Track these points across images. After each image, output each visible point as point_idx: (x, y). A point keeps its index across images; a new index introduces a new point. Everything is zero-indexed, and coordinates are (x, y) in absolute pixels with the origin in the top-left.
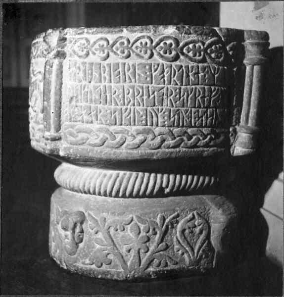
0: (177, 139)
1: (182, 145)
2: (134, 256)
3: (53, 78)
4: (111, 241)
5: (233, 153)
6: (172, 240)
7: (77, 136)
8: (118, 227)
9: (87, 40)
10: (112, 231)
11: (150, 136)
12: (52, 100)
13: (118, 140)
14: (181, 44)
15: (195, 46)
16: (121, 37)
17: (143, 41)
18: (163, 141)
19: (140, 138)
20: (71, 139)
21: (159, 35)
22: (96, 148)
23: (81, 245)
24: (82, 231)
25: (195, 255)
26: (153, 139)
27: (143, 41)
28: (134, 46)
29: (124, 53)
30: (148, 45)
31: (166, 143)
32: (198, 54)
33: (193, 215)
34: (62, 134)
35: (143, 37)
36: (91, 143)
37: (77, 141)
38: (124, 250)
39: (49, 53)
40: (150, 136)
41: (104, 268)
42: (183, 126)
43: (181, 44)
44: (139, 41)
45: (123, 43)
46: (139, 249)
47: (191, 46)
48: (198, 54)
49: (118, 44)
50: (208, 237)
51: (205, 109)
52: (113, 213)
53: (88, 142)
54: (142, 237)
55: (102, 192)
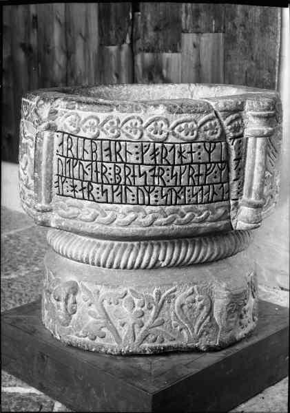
0: (169, 217)
1: (175, 222)
2: (129, 331)
3: (44, 149)
5: (235, 227)
6: (169, 314)
7: (68, 210)
8: (112, 301)
10: (106, 304)
11: (141, 214)
12: (43, 172)
13: (109, 216)
15: (187, 126)
16: (112, 117)
18: (155, 219)
19: (132, 215)
20: (61, 211)
21: (150, 115)
23: (75, 316)
26: (144, 217)
27: (134, 121)
28: (125, 125)
29: (113, 132)
30: (138, 126)
31: (158, 221)
32: (190, 134)
33: (193, 289)
34: (53, 205)
35: (133, 117)
37: (69, 215)
39: (40, 125)
40: (141, 214)
41: (98, 341)
42: (176, 204)
43: (172, 125)
44: (129, 122)
46: (134, 324)
47: (183, 125)
48: (190, 134)
49: (108, 124)
50: (210, 311)
51: (200, 187)
53: (79, 217)
54: (137, 312)
55: (95, 262)
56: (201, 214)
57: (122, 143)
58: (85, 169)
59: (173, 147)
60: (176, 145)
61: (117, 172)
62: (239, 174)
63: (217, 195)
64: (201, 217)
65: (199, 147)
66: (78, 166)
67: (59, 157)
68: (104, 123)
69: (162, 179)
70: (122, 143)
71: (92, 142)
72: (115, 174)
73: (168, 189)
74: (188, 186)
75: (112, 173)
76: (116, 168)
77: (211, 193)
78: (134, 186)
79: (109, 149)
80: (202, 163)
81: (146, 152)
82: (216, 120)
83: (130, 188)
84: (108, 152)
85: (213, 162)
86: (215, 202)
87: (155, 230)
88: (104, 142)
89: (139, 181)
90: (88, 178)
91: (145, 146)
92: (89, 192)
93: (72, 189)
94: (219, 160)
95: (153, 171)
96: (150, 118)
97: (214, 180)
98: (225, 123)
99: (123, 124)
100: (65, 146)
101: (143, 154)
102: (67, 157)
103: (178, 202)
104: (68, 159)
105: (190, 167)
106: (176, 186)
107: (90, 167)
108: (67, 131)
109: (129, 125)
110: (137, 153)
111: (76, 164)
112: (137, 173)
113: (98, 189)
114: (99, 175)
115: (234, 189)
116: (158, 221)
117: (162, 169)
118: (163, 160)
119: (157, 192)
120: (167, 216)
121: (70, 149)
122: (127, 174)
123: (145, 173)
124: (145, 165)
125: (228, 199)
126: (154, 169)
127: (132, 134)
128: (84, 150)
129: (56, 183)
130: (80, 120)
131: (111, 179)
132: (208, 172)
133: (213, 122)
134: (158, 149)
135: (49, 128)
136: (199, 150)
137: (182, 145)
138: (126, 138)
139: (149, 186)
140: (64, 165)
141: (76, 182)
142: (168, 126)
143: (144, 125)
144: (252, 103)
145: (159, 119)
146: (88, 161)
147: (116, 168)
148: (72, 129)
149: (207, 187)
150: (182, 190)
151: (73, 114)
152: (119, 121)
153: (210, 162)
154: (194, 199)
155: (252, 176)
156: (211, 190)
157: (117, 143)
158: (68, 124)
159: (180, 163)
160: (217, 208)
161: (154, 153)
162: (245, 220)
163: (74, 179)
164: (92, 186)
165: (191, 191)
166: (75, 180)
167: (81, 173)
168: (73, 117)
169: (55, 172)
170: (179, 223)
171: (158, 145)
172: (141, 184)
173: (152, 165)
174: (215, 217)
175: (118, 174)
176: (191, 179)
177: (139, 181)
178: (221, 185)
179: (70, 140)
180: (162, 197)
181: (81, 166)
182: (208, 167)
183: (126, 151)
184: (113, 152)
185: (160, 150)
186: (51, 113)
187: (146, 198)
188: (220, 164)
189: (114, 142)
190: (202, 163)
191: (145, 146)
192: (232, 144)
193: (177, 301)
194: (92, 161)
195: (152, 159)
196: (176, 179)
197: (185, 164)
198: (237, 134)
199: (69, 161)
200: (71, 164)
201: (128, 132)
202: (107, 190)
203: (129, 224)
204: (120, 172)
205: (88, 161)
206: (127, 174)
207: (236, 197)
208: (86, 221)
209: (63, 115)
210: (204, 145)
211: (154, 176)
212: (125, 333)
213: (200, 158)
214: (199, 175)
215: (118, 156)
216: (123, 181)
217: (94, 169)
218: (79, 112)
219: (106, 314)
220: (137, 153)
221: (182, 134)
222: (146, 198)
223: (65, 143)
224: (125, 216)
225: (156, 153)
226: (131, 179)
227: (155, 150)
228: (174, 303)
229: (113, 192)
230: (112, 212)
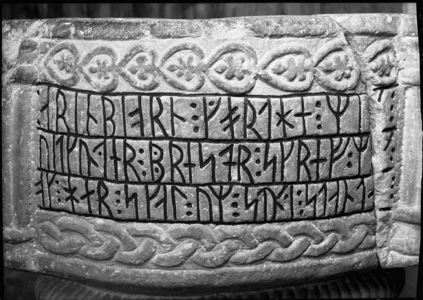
0: (261, 246)
7: (61, 238)
9: (73, 50)
13: (140, 249)
15: (291, 62)
18: (232, 251)
19: (188, 245)
22: (97, 265)
26: (209, 249)
27: (185, 55)
36: (89, 252)
42: (273, 221)
43: (262, 61)
44: (178, 55)
45: (142, 59)
47: (283, 61)
48: (299, 77)
49: (133, 62)
56: (322, 240)
57: (164, 99)
58: (90, 152)
59: (268, 104)
60: (273, 100)
61: (155, 157)
62: (391, 159)
63: (352, 200)
64: (322, 244)
65: (318, 104)
66: (76, 149)
67: (40, 132)
68: (126, 60)
69: (246, 169)
70: (164, 99)
71: (103, 99)
72: (152, 162)
73: (256, 189)
74: (298, 182)
75: (147, 161)
77: (341, 196)
78: (190, 185)
79: (139, 111)
80: (325, 136)
83: (183, 189)
84: (137, 117)
85: (344, 135)
86: (350, 214)
87: (233, 273)
90: (99, 171)
91: (211, 103)
92: (101, 200)
93: (68, 195)
94: (356, 131)
95: (228, 154)
96: (220, 47)
97: (347, 171)
101: (206, 119)
102: (57, 133)
103: (278, 216)
105: (301, 144)
106: (274, 183)
107: (101, 149)
108: (55, 82)
109: (177, 63)
111: (74, 146)
112: (195, 158)
113: (118, 192)
114: (120, 167)
116: (241, 254)
117: (247, 150)
118: (248, 130)
119: (236, 195)
120: (256, 246)
121: (62, 116)
122: (175, 161)
123: (212, 158)
125: (371, 209)
126: (230, 149)
127: (182, 81)
128: (89, 115)
129: (36, 185)
130: (78, 59)
132: (336, 155)
133: (341, 55)
134: (236, 108)
136: (317, 110)
137: (284, 100)
138: (170, 90)
139: (221, 184)
141: (76, 181)
142: (256, 63)
143: (206, 61)
146: (98, 137)
147: (154, 149)
148: (64, 76)
149: (335, 183)
150: (287, 191)
152: (153, 54)
154: (309, 208)
156: (342, 190)
157: (155, 98)
158: (55, 68)
159: (281, 136)
160: (355, 225)
161: (229, 117)
163: (70, 175)
164: (106, 188)
165: (303, 193)
166: (72, 178)
167: (85, 164)
168: (66, 53)
170: (280, 260)
171: (236, 101)
172: (202, 182)
175: (158, 162)
176: (302, 167)
177: (202, 174)
178: (359, 180)
179: (61, 98)
180: (248, 206)
181: (83, 148)
183: (173, 115)
185: (240, 111)
186: (23, 47)
187: (216, 209)
188: (357, 139)
190: (325, 136)
192: (379, 100)
194: (105, 137)
195: (225, 129)
196: (274, 168)
197: (292, 139)
198: (386, 80)
199: (61, 139)
201: (172, 76)
202: (135, 195)
203: (181, 264)
204: (161, 157)
205: (98, 137)
206: (175, 161)
207: (385, 205)
208: (96, 259)
209: (46, 51)
210: (328, 99)
211: (229, 163)
213: (319, 127)
214: (318, 161)
215: (156, 125)
216: (167, 176)
217: (110, 153)
218: (78, 44)
221: (282, 80)
222: (216, 209)
223: (52, 105)
224: (174, 246)
225: (233, 117)
226: (185, 170)
227: (232, 110)
229: (149, 199)
230: (146, 240)
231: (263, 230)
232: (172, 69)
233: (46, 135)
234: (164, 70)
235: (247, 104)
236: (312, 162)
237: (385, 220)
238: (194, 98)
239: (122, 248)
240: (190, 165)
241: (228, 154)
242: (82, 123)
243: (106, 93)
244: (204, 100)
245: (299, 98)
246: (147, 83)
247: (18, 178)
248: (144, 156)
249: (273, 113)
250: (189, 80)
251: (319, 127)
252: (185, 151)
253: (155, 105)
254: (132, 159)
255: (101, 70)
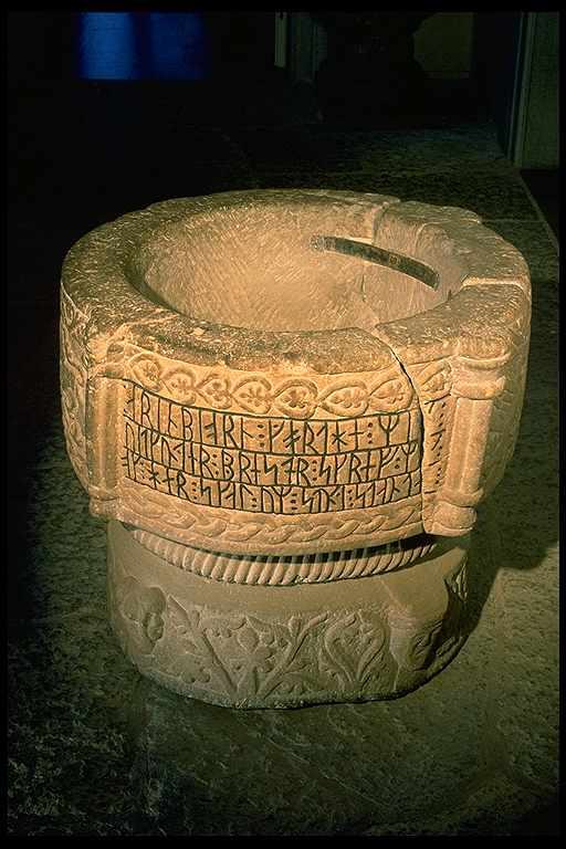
2: (247, 677)
4: (207, 650)
6: (315, 654)
10: (210, 632)
14: (320, 394)
16: (215, 375)
17: (255, 386)
18: (290, 533)
19: (253, 527)
24: (160, 624)
25: (358, 677)
27: (255, 386)
30: (263, 394)
31: (297, 535)
38: (229, 664)
41: (198, 685)
45: (217, 385)
46: (255, 671)
47: (340, 393)
49: (210, 385)
50: (385, 642)
52: (213, 609)
57: (234, 417)
59: (325, 427)
65: (370, 425)
66: (159, 444)
68: (203, 383)
69: (303, 475)
70: (234, 417)
71: (183, 410)
73: (313, 490)
75: (219, 464)
76: (225, 456)
81: (276, 435)
82: (402, 378)
83: (249, 487)
88: (203, 413)
89: (266, 479)
91: (275, 426)
95: (289, 464)
96: (284, 381)
97: (395, 472)
98: (416, 381)
99: (238, 387)
100: (138, 408)
101: (271, 438)
104: (142, 429)
105: (353, 456)
106: (328, 485)
107: (181, 449)
110: (261, 436)
111: (157, 441)
112: (260, 466)
114: (196, 465)
115: (429, 477)
116: (297, 535)
117: (303, 460)
124: (274, 454)
126: (291, 461)
127: (251, 406)
131: (217, 473)
133: (394, 383)
134: (297, 431)
135: (108, 374)
137: (340, 423)
140: (136, 436)
143: (272, 392)
144: (468, 344)
145: (300, 383)
147: (225, 456)
148: (151, 384)
150: (339, 491)
151: (147, 357)
153: (387, 446)
154: (359, 501)
155: (461, 457)
157: (227, 417)
161: (291, 436)
162: (447, 524)
167: (166, 457)
169: (122, 441)
170: (332, 537)
173: (287, 455)
174: (394, 522)
175: (229, 466)
176: (353, 473)
177: (266, 479)
179: (145, 398)
180: (304, 503)
182: (384, 454)
183: (242, 431)
184: (220, 431)
185: (301, 433)
187: (277, 504)
189: (222, 415)
191: (275, 426)
193: (328, 633)
198: (439, 394)
200: (149, 439)
209: (132, 355)
211: (290, 471)
212: (242, 679)
213: (370, 442)
216: (236, 476)
217: (187, 449)
218: (162, 360)
219: (211, 650)
220: (261, 436)
221: (339, 407)
222: (277, 504)
223: (137, 402)
225: (295, 437)
226: (252, 474)
227: (293, 433)
228: (323, 635)
229: (220, 493)
231: (317, 519)
232: (243, 396)
233: (132, 423)
234: (236, 395)
235: (306, 427)
236: (362, 469)
237: (429, 501)
238: (261, 421)
239: (198, 522)
240: (255, 471)
241: (289, 464)
242: (164, 426)
243: (185, 406)
244: (270, 423)
245: (354, 421)
246: (221, 404)
247: (106, 453)
248: (219, 458)
249: (329, 434)
250: (257, 406)
251: (370, 442)
252: (252, 461)
253: (228, 422)
254: (207, 461)
255: (183, 387)
